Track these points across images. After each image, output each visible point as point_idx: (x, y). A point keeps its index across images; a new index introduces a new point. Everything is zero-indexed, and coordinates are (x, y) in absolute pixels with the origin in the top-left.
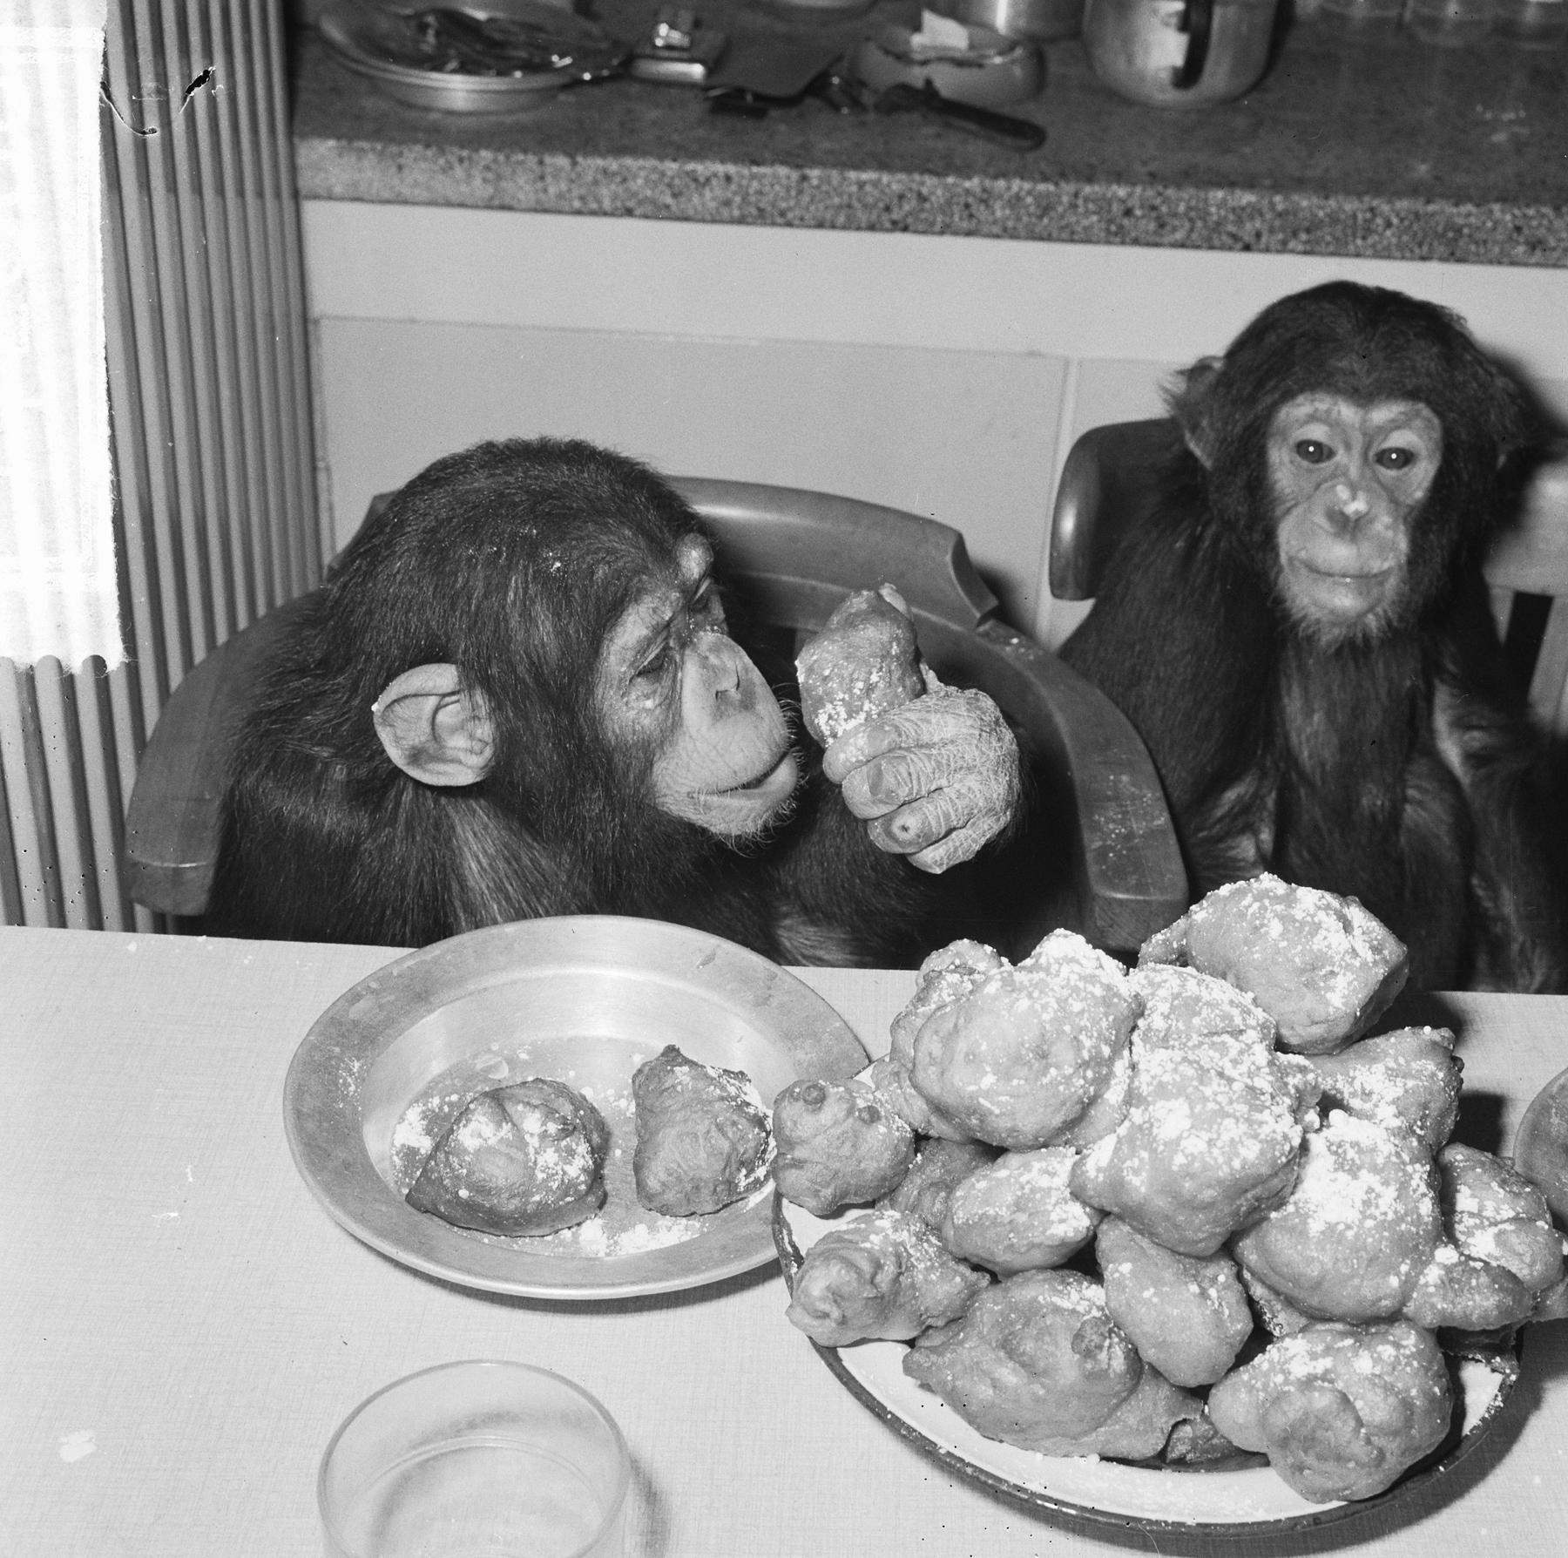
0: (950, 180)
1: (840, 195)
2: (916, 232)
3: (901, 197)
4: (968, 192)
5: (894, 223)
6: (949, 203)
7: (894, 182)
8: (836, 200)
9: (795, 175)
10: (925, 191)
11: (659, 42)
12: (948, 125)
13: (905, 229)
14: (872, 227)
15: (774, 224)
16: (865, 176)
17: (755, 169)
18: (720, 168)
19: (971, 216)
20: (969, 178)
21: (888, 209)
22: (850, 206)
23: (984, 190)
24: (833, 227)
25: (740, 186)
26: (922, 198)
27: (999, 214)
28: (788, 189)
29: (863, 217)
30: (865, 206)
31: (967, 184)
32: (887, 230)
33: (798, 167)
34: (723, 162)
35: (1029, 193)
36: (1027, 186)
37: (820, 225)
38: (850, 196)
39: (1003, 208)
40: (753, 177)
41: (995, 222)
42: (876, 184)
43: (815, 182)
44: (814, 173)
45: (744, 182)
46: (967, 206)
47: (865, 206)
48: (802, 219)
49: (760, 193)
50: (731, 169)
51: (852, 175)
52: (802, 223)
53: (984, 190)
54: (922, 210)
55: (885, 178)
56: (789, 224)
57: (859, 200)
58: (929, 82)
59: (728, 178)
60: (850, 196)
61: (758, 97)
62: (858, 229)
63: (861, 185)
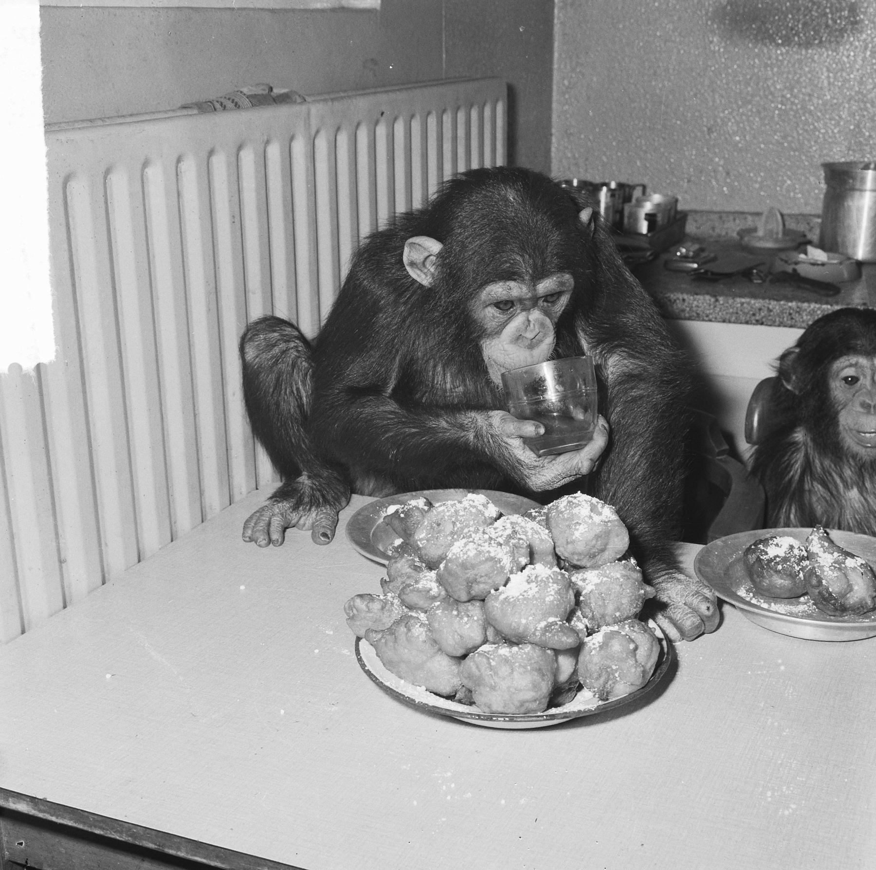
0: (782, 302)
1: (733, 308)
2: (766, 325)
3: (760, 309)
4: (790, 307)
5: (757, 321)
6: (782, 312)
7: (757, 303)
8: (731, 310)
9: (713, 300)
10: (771, 307)
11: (678, 254)
12: (799, 287)
13: (762, 324)
14: (747, 323)
15: (703, 320)
16: (743, 300)
17: (695, 296)
18: (681, 296)
19: (792, 319)
20: (791, 301)
21: (754, 315)
22: (737, 313)
23: (798, 307)
24: (730, 322)
25: (689, 303)
26: (770, 310)
27: (805, 318)
28: (710, 305)
29: (743, 318)
30: (744, 313)
31: (790, 304)
32: (754, 324)
33: (715, 296)
34: (682, 293)
35: (819, 309)
36: (817, 306)
37: (724, 321)
38: (737, 308)
39: (807, 315)
40: (694, 300)
41: (803, 322)
42: (749, 303)
43: (721, 302)
44: (721, 299)
45: (691, 302)
46: (790, 314)
47: (744, 313)
48: (716, 318)
49: (697, 306)
50: (685, 296)
51: (738, 300)
52: (716, 320)
53: (798, 307)
54: (770, 316)
55: (753, 302)
56: (710, 321)
57: (741, 310)
58: (795, 270)
59: (684, 300)
60: (737, 308)
61: (713, 273)
62: (741, 323)
63: (742, 304)
